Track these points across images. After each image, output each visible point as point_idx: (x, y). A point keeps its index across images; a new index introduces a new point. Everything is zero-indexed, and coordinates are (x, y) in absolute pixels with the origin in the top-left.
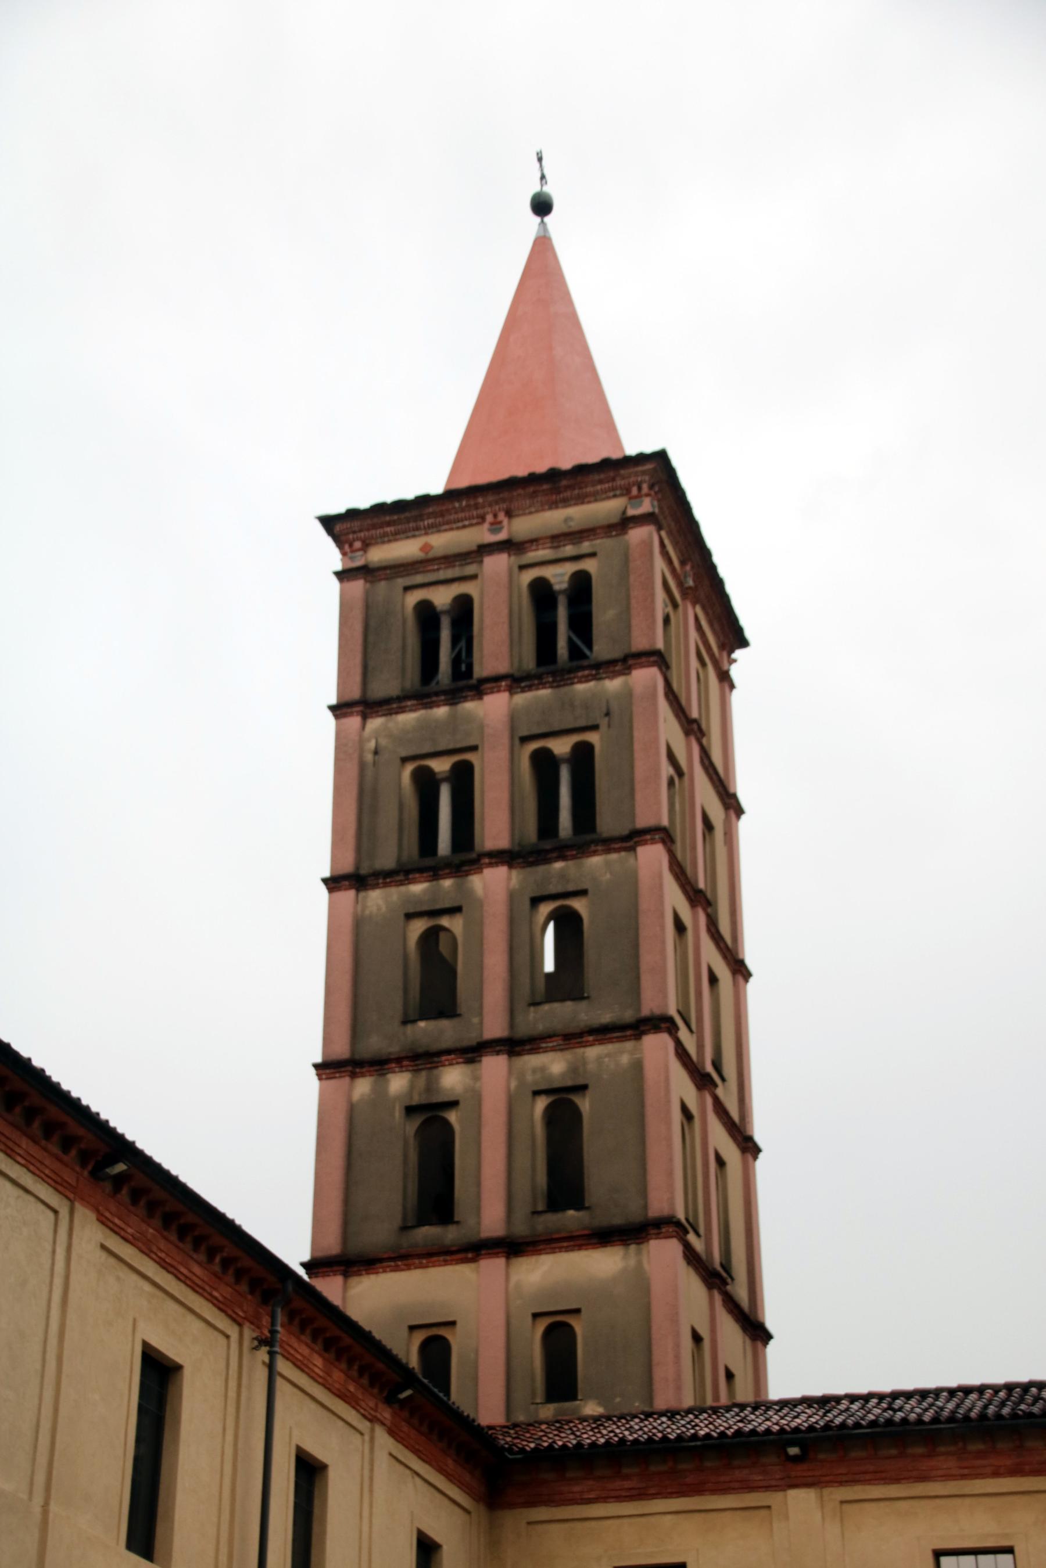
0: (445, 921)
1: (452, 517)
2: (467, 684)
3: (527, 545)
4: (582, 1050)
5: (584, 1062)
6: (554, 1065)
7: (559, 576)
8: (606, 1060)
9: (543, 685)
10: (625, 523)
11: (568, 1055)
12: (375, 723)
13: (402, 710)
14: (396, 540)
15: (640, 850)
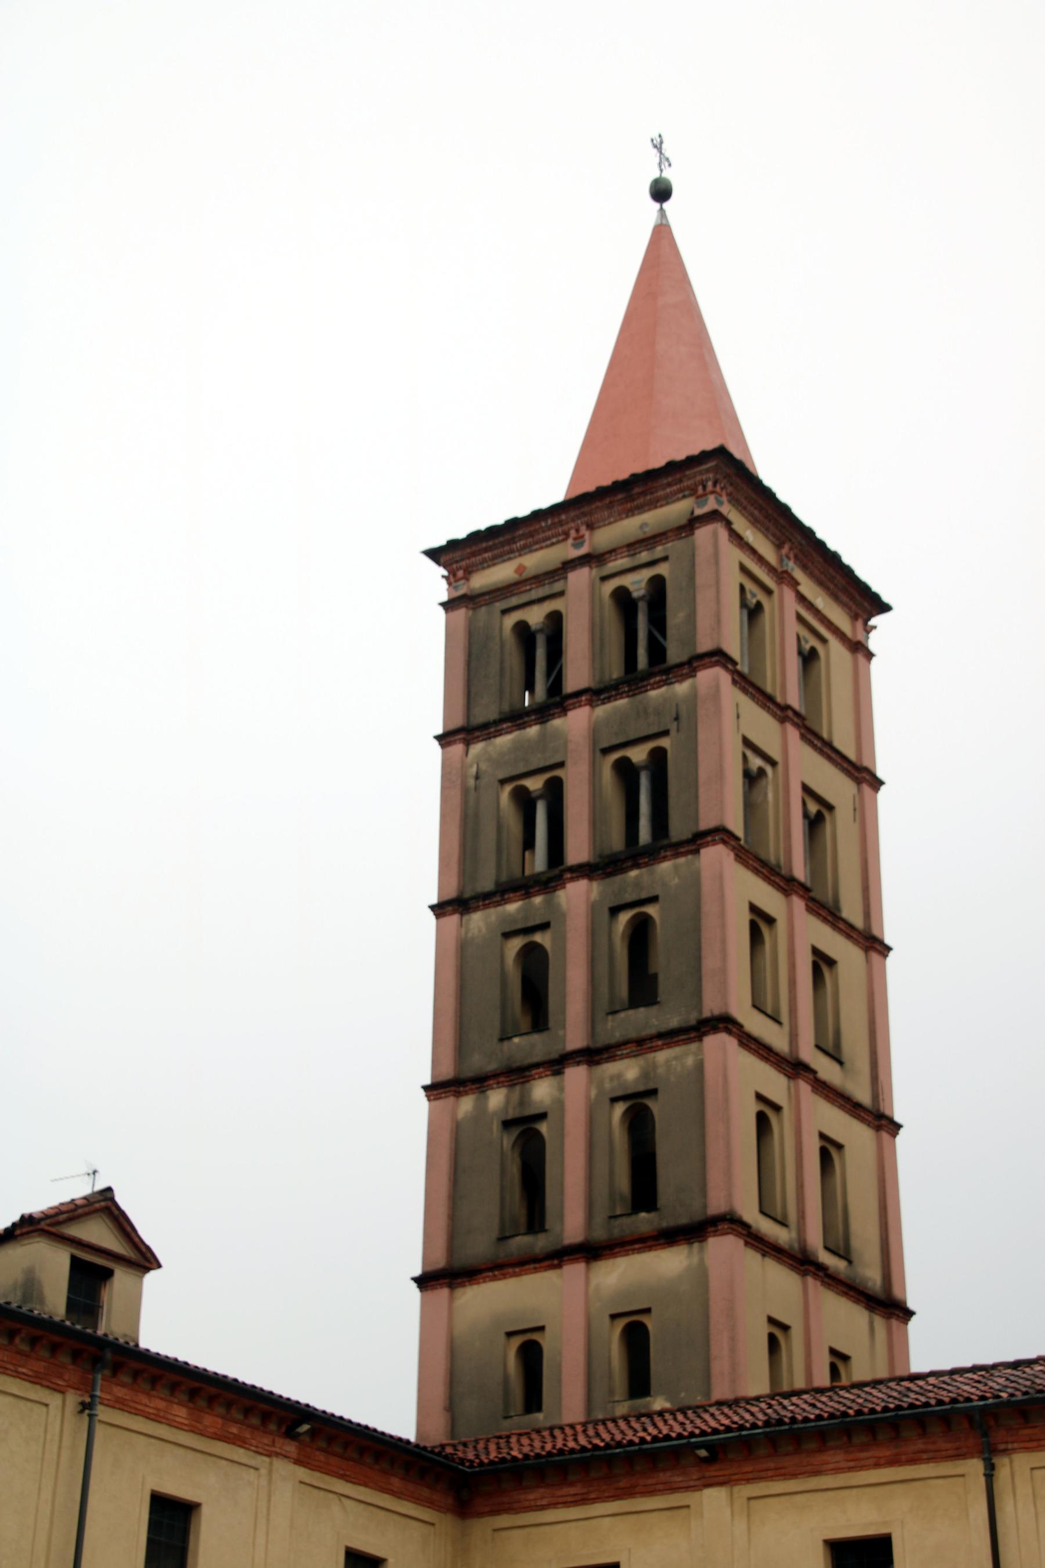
0: (538, 938)
1: (541, 536)
2: (558, 701)
3: (607, 556)
4: (652, 1055)
5: (655, 1066)
6: (628, 1071)
7: (637, 583)
8: (674, 1063)
9: (620, 696)
10: (692, 523)
11: (641, 1061)
12: (477, 748)
13: (499, 733)
14: (494, 565)
15: (703, 851)
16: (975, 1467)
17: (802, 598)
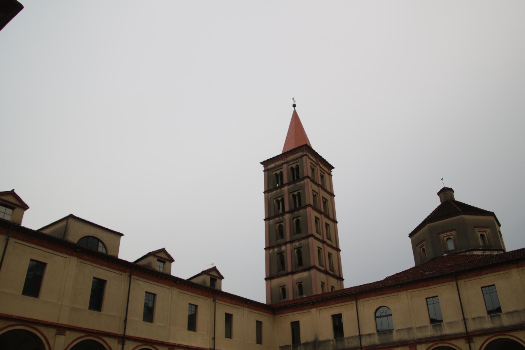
0: (281, 223)
2: (282, 185)
6: (297, 244)
7: (294, 166)
10: (302, 156)
12: (270, 194)
16: (354, 302)
17: (320, 167)
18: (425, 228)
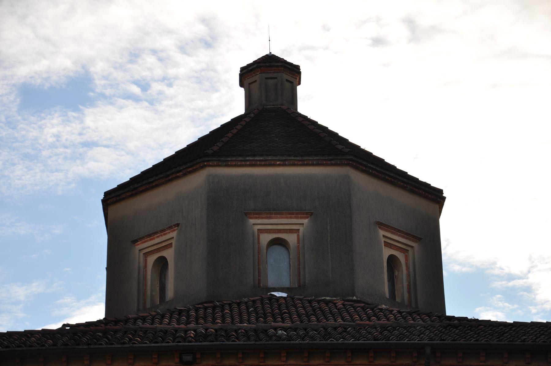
18: (196, 181)
